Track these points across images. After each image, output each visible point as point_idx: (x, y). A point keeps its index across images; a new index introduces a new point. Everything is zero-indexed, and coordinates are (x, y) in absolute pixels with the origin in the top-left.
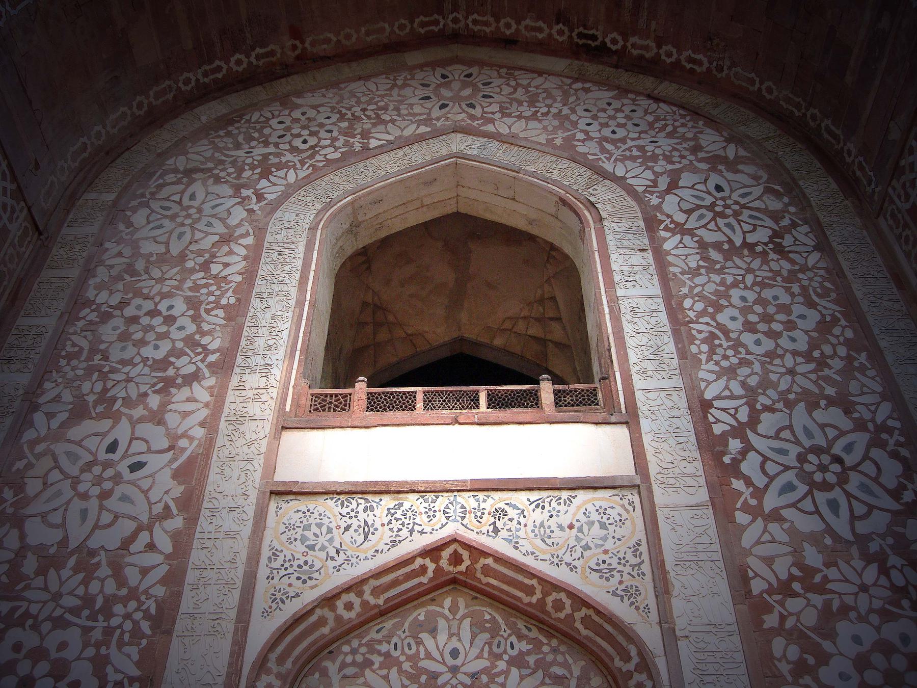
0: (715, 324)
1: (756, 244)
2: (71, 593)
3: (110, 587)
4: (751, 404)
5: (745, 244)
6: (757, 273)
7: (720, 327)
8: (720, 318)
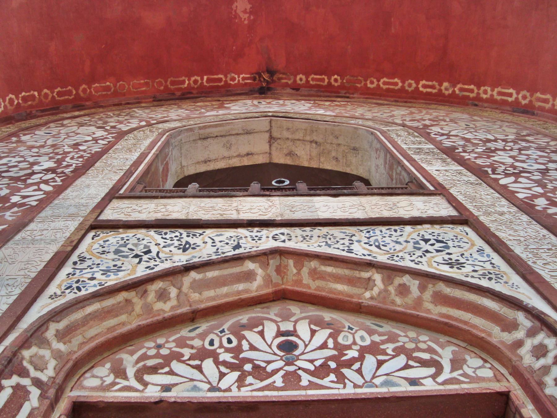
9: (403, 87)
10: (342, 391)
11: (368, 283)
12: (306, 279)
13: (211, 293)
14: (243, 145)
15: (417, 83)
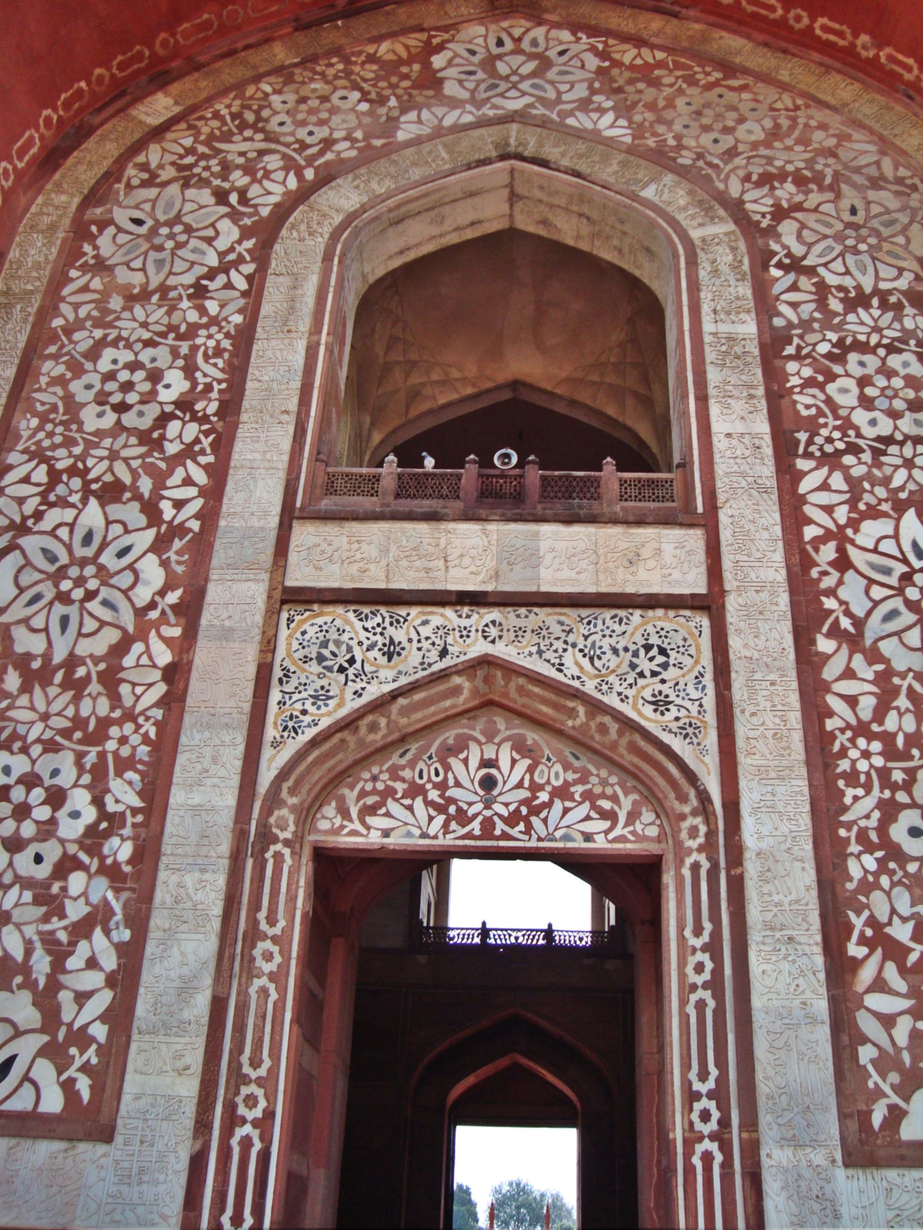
0: (823, 397)
1: (890, 292)
3: (103, 707)
4: (852, 503)
5: (876, 291)
6: (885, 332)
7: (829, 401)
8: (831, 388)
9: (784, 19)
10: (528, 845)
11: (572, 713)
12: (513, 694)
13: (418, 715)
14: (464, 213)
15: (813, 19)
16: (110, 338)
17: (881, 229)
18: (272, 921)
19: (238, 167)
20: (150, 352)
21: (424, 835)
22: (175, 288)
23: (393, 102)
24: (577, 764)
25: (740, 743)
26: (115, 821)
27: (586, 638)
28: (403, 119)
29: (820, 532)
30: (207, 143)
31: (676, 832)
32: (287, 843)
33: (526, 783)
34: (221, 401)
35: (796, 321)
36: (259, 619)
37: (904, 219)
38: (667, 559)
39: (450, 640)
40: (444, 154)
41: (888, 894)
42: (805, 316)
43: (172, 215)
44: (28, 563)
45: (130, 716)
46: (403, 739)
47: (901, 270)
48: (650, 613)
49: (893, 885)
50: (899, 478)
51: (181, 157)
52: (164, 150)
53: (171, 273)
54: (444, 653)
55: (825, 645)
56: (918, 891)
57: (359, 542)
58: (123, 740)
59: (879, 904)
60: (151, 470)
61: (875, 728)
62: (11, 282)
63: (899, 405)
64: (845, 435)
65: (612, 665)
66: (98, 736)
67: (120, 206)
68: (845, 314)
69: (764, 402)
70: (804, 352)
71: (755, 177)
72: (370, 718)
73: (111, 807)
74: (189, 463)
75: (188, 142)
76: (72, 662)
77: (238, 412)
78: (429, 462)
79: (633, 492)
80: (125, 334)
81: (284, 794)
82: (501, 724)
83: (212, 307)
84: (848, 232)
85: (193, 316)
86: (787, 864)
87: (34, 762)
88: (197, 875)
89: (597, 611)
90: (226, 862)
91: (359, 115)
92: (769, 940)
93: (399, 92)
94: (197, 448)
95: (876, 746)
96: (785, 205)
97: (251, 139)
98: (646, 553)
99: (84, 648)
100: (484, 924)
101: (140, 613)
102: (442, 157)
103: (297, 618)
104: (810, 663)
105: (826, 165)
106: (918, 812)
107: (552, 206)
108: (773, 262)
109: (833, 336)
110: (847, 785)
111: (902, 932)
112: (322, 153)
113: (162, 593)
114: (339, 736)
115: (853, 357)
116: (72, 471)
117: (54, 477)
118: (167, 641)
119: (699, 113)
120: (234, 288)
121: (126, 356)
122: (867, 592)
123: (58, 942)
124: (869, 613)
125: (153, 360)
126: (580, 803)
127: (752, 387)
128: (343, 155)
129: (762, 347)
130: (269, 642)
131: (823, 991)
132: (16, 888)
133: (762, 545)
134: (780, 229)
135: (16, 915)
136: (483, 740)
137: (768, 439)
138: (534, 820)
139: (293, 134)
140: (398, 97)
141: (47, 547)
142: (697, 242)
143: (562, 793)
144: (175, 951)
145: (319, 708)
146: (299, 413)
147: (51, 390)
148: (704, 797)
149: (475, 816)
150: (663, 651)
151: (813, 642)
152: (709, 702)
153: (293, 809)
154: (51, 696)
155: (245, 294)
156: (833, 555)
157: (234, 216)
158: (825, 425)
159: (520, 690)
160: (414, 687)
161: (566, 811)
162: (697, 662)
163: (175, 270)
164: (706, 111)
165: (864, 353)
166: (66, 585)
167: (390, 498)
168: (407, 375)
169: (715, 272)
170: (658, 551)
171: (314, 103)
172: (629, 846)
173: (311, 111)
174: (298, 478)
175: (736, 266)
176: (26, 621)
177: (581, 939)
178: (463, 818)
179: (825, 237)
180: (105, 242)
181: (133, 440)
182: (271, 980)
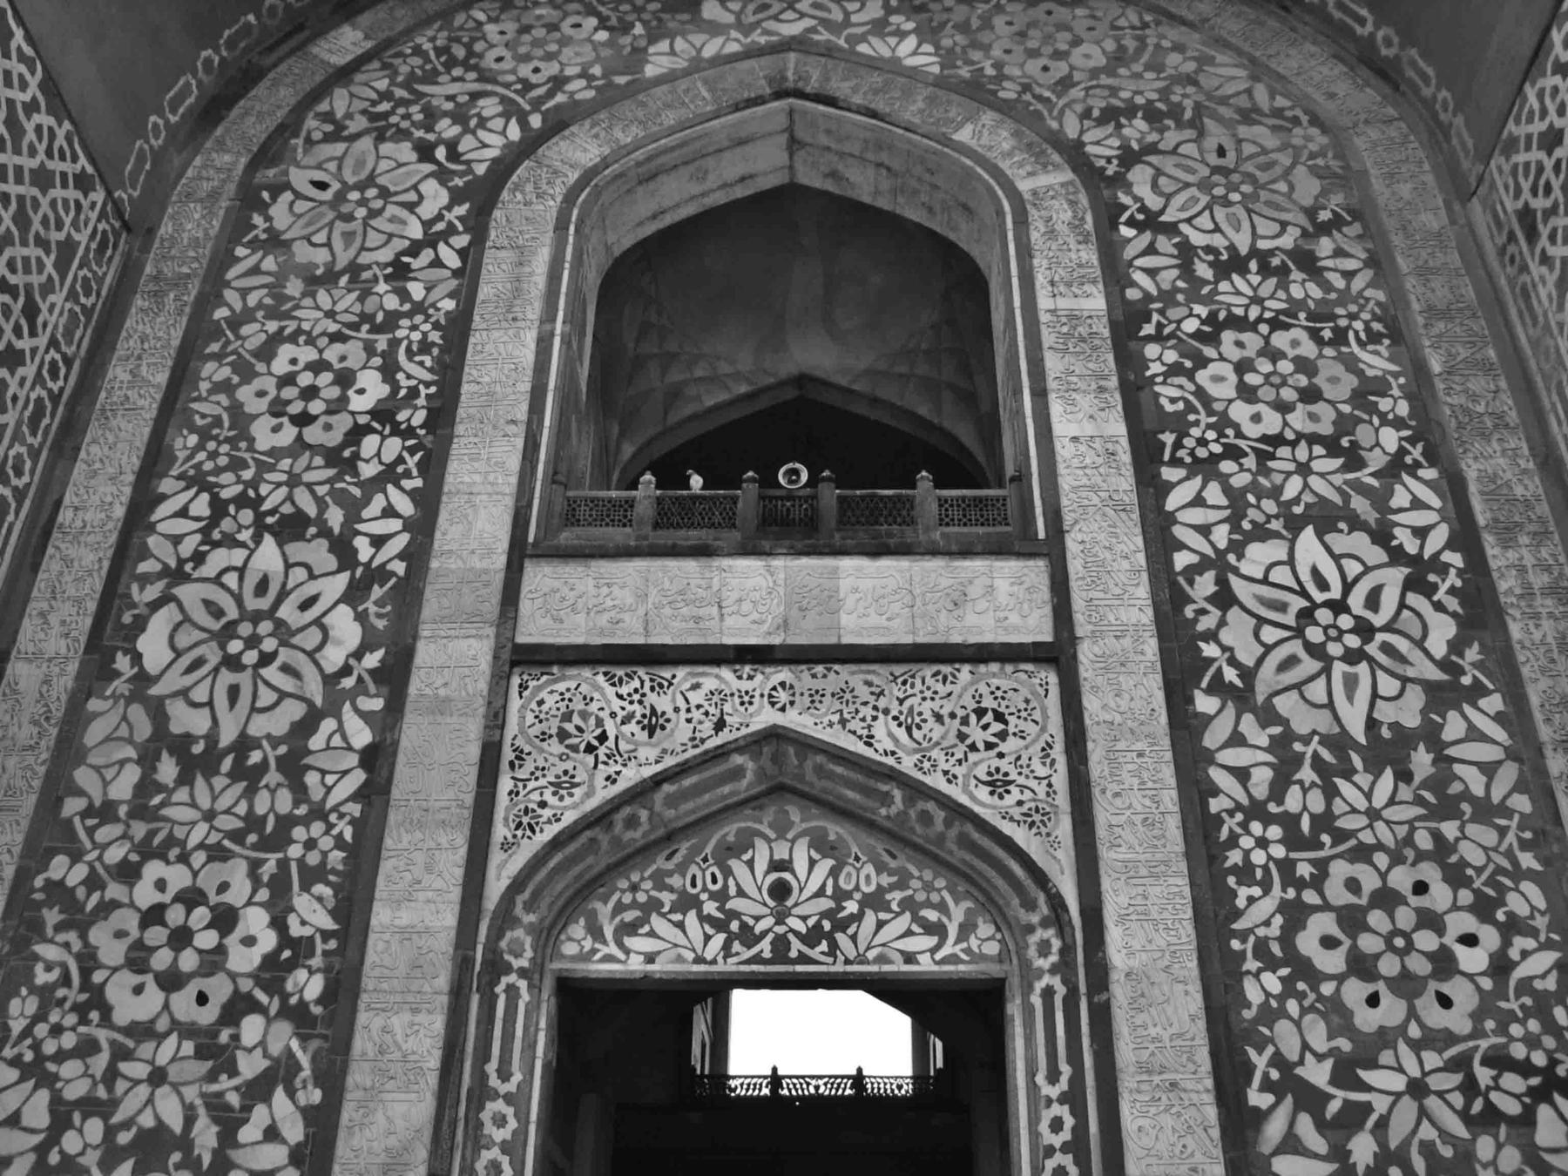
0: (1192, 388)
1: (1272, 252)
2: (228, 812)
4: (1234, 521)
5: (1254, 252)
6: (1268, 304)
7: (1200, 392)
8: (1202, 377)
10: (833, 969)
12: (810, 776)
13: (690, 805)
14: (730, 167)
16: (287, 332)
17: (1258, 173)
18: (504, 1075)
19: (446, 114)
20: (338, 348)
21: (699, 960)
22: (369, 267)
23: (639, 29)
24: (893, 864)
25: (1101, 832)
26: (300, 949)
27: (901, 702)
28: (651, 50)
29: (1194, 559)
30: (406, 85)
31: (1022, 949)
32: (523, 973)
33: (829, 891)
34: (429, 410)
35: (1155, 293)
36: (483, 686)
37: (1285, 159)
38: (999, 598)
39: (727, 708)
40: (705, 94)
41: (1298, 1024)
42: (1166, 286)
43: (363, 175)
44: (187, 619)
45: (319, 813)
46: (671, 837)
47: (1284, 225)
48: (982, 668)
49: (1304, 1011)
50: (1293, 488)
51: (374, 103)
52: (352, 95)
53: (363, 248)
54: (720, 725)
55: (1205, 703)
56: (1336, 1019)
57: (608, 585)
58: (310, 844)
59: (1286, 1037)
60: (341, 498)
61: (1273, 808)
62: (162, 265)
63: (1288, 394)
64: (1221, 435)
65: (936, 736)
66: (279, 840)
67: (298, 166)
68: (1216, 282)
69: (1118, 396)
70: (1167, 331)
71: (1096, 113)
72: (626, 811)
73: (296, 930)
74: (390, 488)
75: (382, 85)
76: (244, 744)
77: (452, 423)
78: (696, 481)
79: (956, 513)
80: (306, 326)
81: (519, 910)
82: (795, 815)
83: (416, 290)
84: (1216, 178)
85: (392, 302)
86: (1166, 988)
87: (195, 874)
88: (407, 1017)
89: (914, 667)
90: (445, 999)
91: (595, 46)
92: (1144, 1087)
93: (646, 16)
94: (400, 469)
95: (1275, 832)
96: (1135, 146)
97: (460, 79)
98: (975, 591)
99: (259, 726)
100: (775, 1069)
101: (330, 680)
102: (702, 96)
103: (532, 684)
104: (1187, 727)
105: (1185, 96)
106: (1333, 915)
107: (842, 155)
108: (1123, 219)
109: (1202, 310)
110: (1239, 883)
111: (1318, 1074)
112: (550, 94)
113: (358, 654)
114: (588, 834)
115: (1228, 337)
116: (241, 501)
117: (219, 509)
118: (364, 716)
119: (1022, 35)
120: (444, 266)
121: (307, 354)
122: (1257, 635)
123: (228, 1108)
124: (1260, 661)
125: (343, 358)
126: (898, 915)
127: (1105, 378)
128: (578, 97)
129: (1113, 325)
130: (496, 715)
131: (1218, 1152)
132: (173, 1039)
133: (1123, 578)
134: (1130, 176)
135: (173, 1073)
136: (773, 835)
137: (1125, 442)
138: (839, 936)
139: (513, 71)
140: (645, 23)
141: (211, 597)
142: (1027, 196)
143: (875, 901)
144: (380, 1117)
145: (561, 798)
146: (529, 422)
147: (214, 398)
148: (1057, 903)
149: (764, 934)
150: (999, 717)
151: (1190, 700)
152: (1061, 780)
153: (531, 929)
154: (218, 789)
155: (457, 273)
156: (1212, 589)
157: (442, 175)
158: (1197, 423)
159: (819, 770)
160: (683, 769)
161: (881, 925)
162: (1043, 730)
163: (368, 244)
164: (1031, 33)
165: (1241, 330)
166: (235, 646)
167: (648, 530)
168: (664, 370)
169: (1051, 234)
170: (990, 589)
171: (539, 33)
172: (962, 968)
173: (536, 43)
174: (530, 505)
175: (1076, 225)
176: (184, 693)
177: (900, 1087)
178: (749, 937)
179: (1187, 185)
180: (280, 213)
181: (318, 461)
182: (504, 1152)
